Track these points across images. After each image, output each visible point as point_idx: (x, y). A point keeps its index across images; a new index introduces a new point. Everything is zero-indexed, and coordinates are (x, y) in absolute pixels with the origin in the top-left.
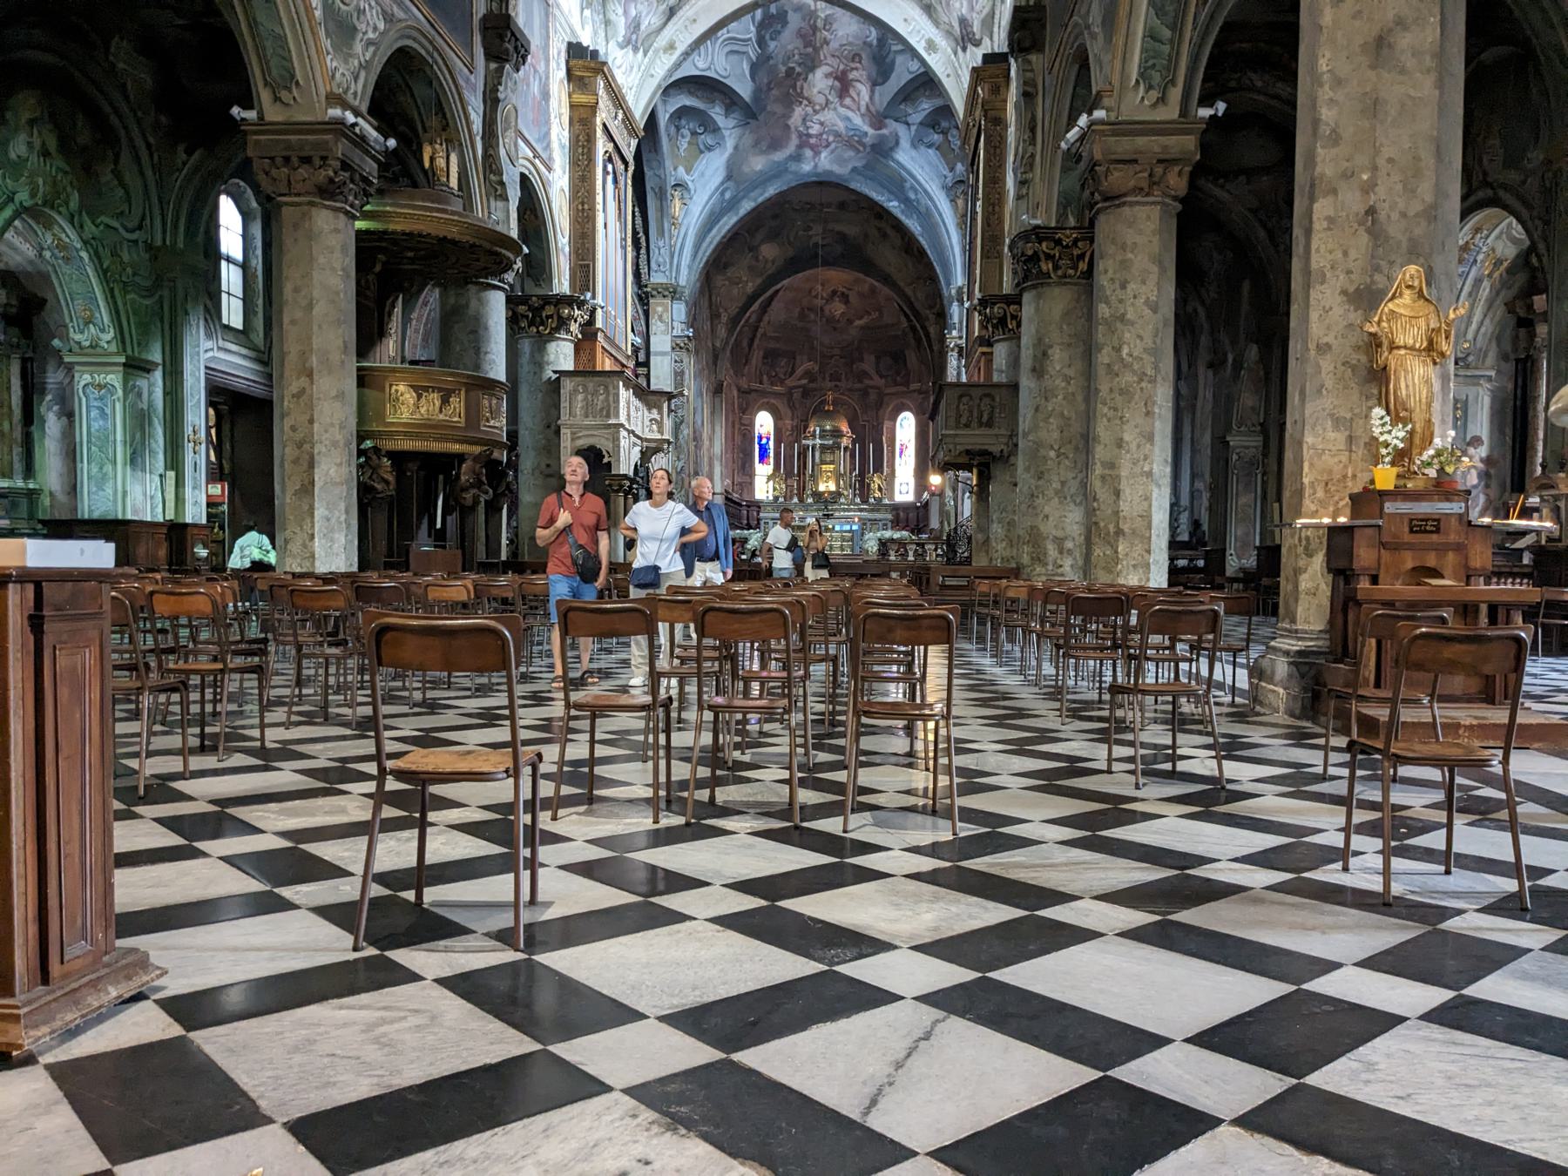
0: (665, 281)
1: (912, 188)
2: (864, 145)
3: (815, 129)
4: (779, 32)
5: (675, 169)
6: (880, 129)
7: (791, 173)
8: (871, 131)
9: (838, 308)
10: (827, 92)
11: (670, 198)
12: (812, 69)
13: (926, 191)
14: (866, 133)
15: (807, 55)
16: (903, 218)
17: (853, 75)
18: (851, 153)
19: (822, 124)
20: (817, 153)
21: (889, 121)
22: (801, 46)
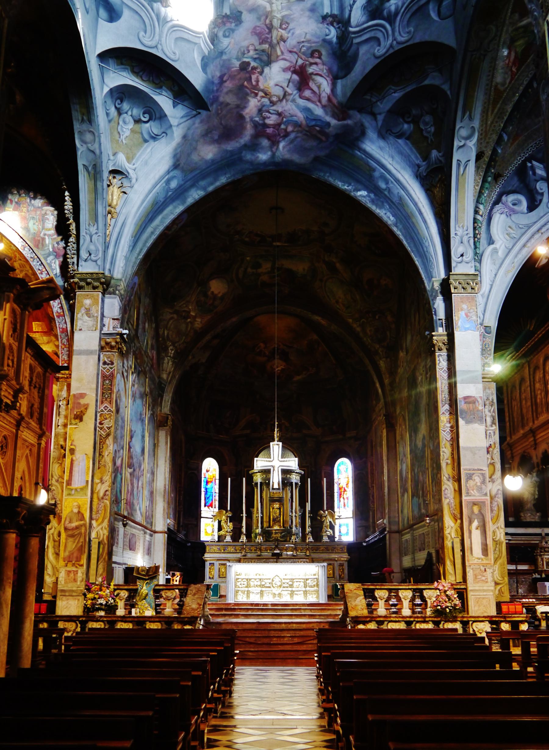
0: (96, 270)
1: (383, 177)
2: (326, 135)
3: (272, 120)
4: (233, 31)
5: (114, 154)
6: (344, 119)
7: (247, 162)
8: (334, 122)
9: (278, 366)
10: (285, 85)
11: (106, 183)
12: (269, 63)
13: (398, 181)
14: (328, 124)
15: (263, 51)
16: (373, 208)
17: (311, 70)
18: (312, 143)
19: (279, 114)
20: (274, 143)
21: (351, 112)
22: (256, 43)
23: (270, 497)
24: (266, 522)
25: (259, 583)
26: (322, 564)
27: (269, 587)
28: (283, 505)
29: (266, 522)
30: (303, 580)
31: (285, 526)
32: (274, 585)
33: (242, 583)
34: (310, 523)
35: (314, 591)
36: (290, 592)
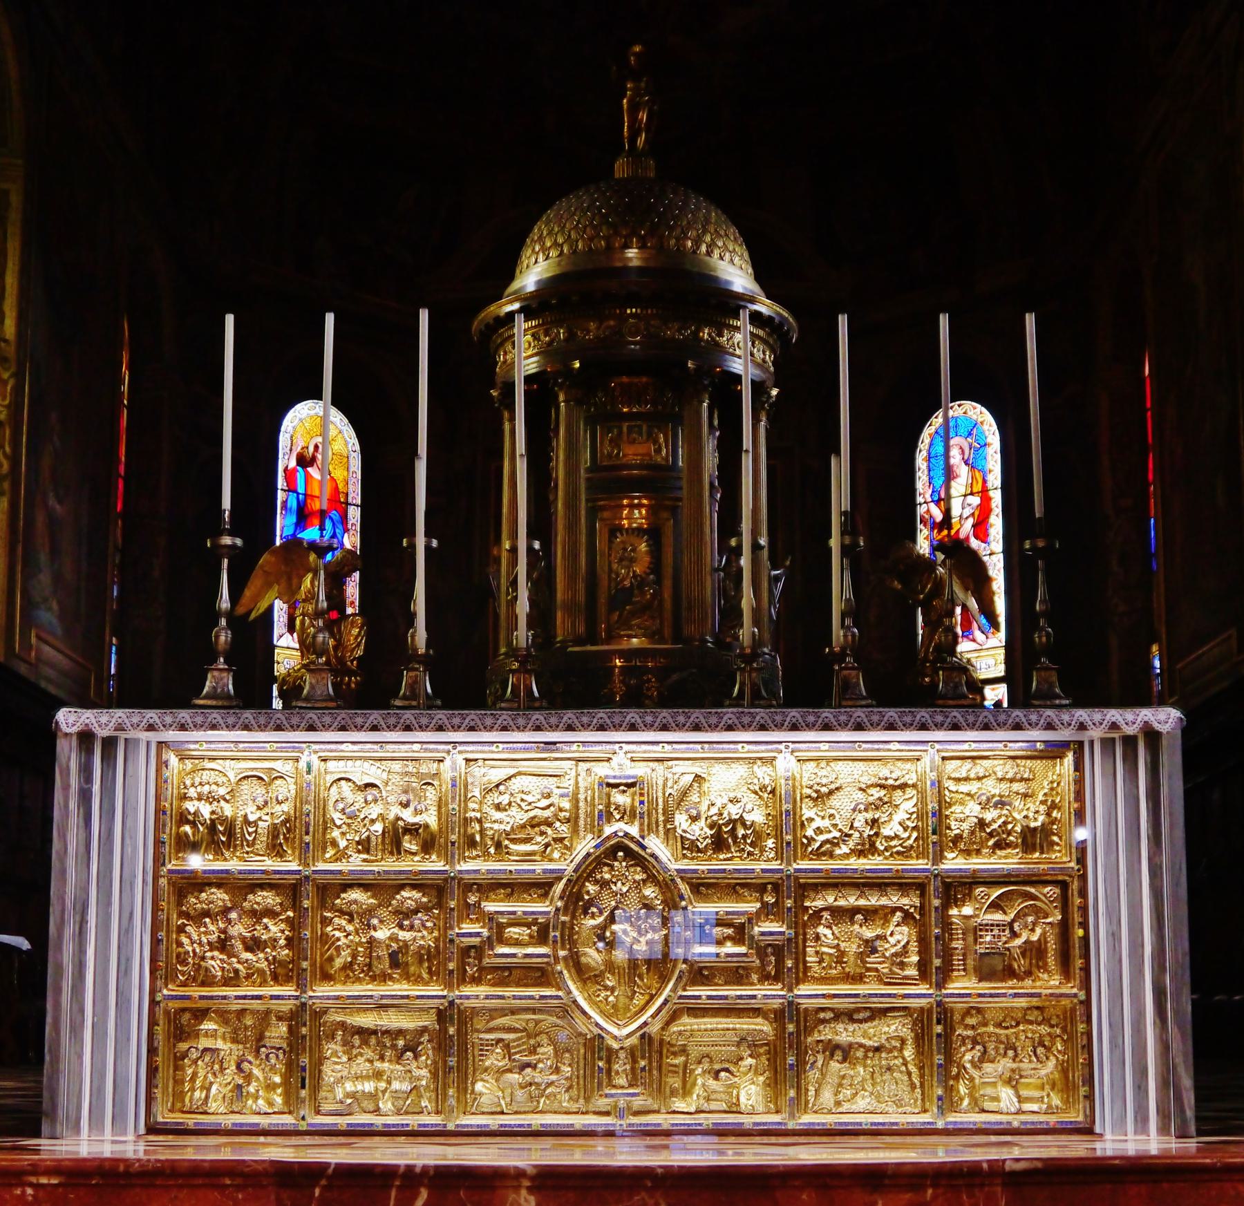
23: (595, 467)
24: (570, 608)
25: (420, 936)
26: (1132, 719)
27: (540, 975)
28: (674, 510)
29: (570, 608)
30: (909, 901)
31: (689, 630)
32: (593, 956)
33: (239, 929)
34: (849, 593)
35: (1041, 1011)
36: (763, 1026)
